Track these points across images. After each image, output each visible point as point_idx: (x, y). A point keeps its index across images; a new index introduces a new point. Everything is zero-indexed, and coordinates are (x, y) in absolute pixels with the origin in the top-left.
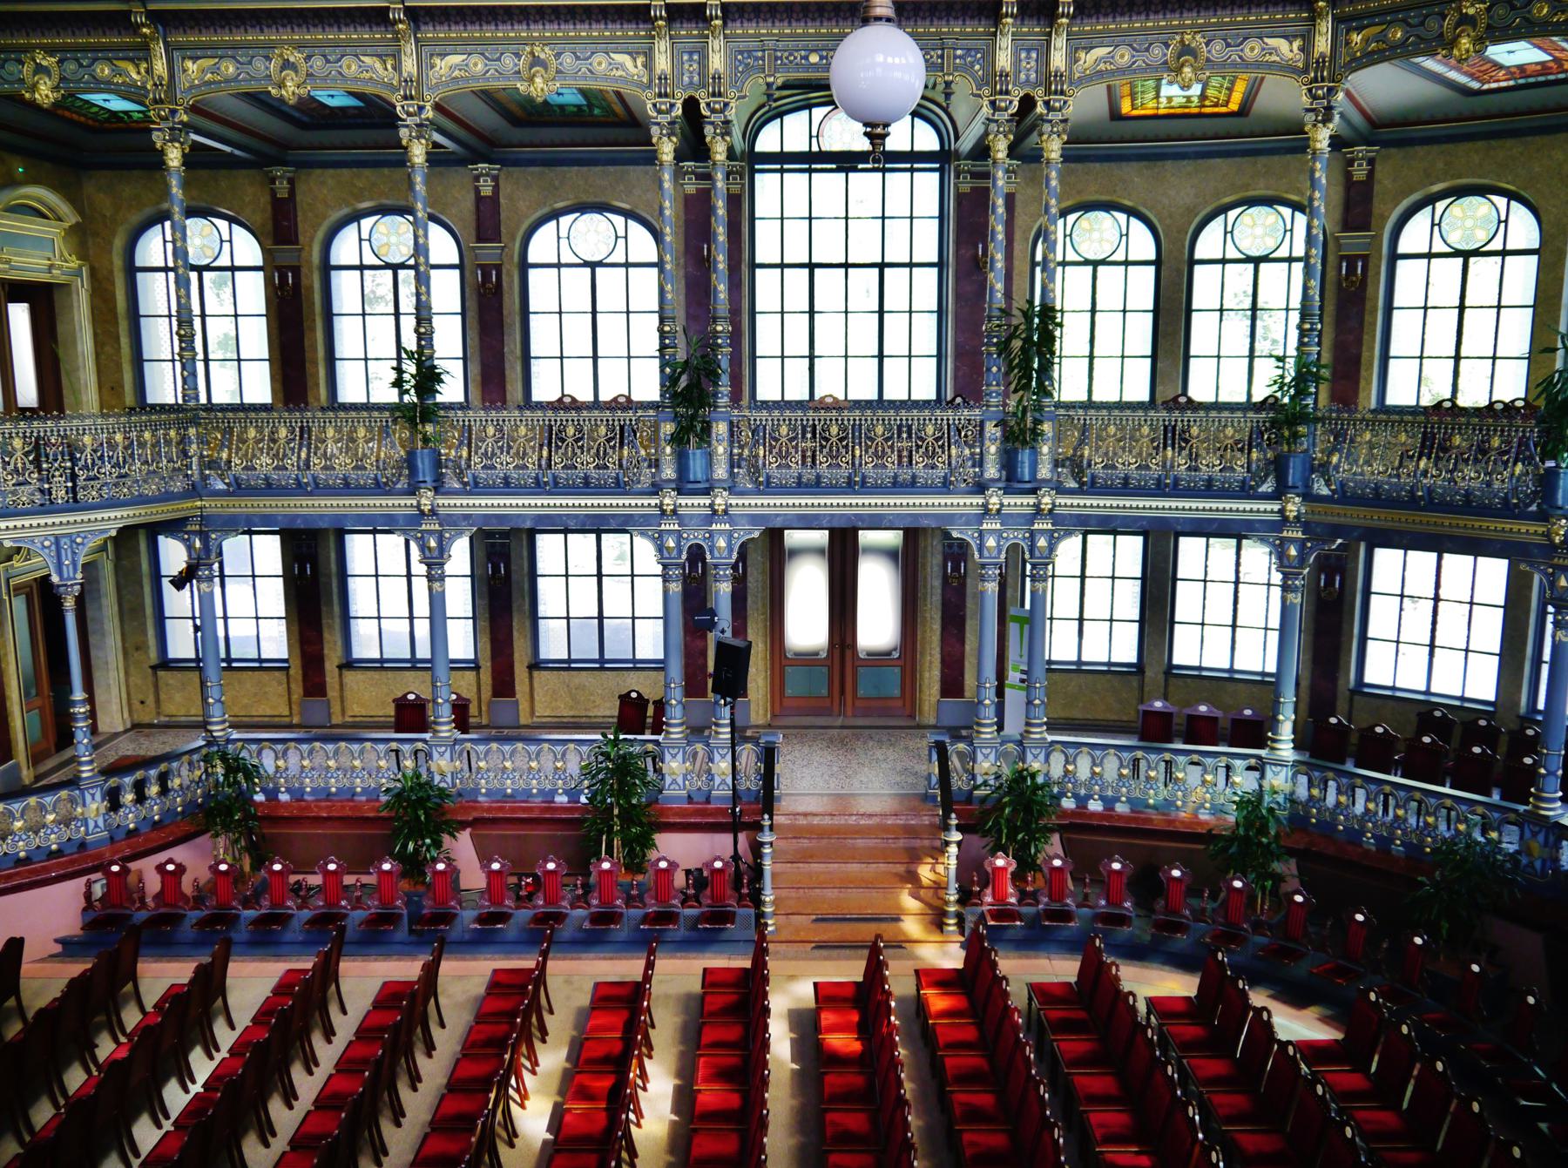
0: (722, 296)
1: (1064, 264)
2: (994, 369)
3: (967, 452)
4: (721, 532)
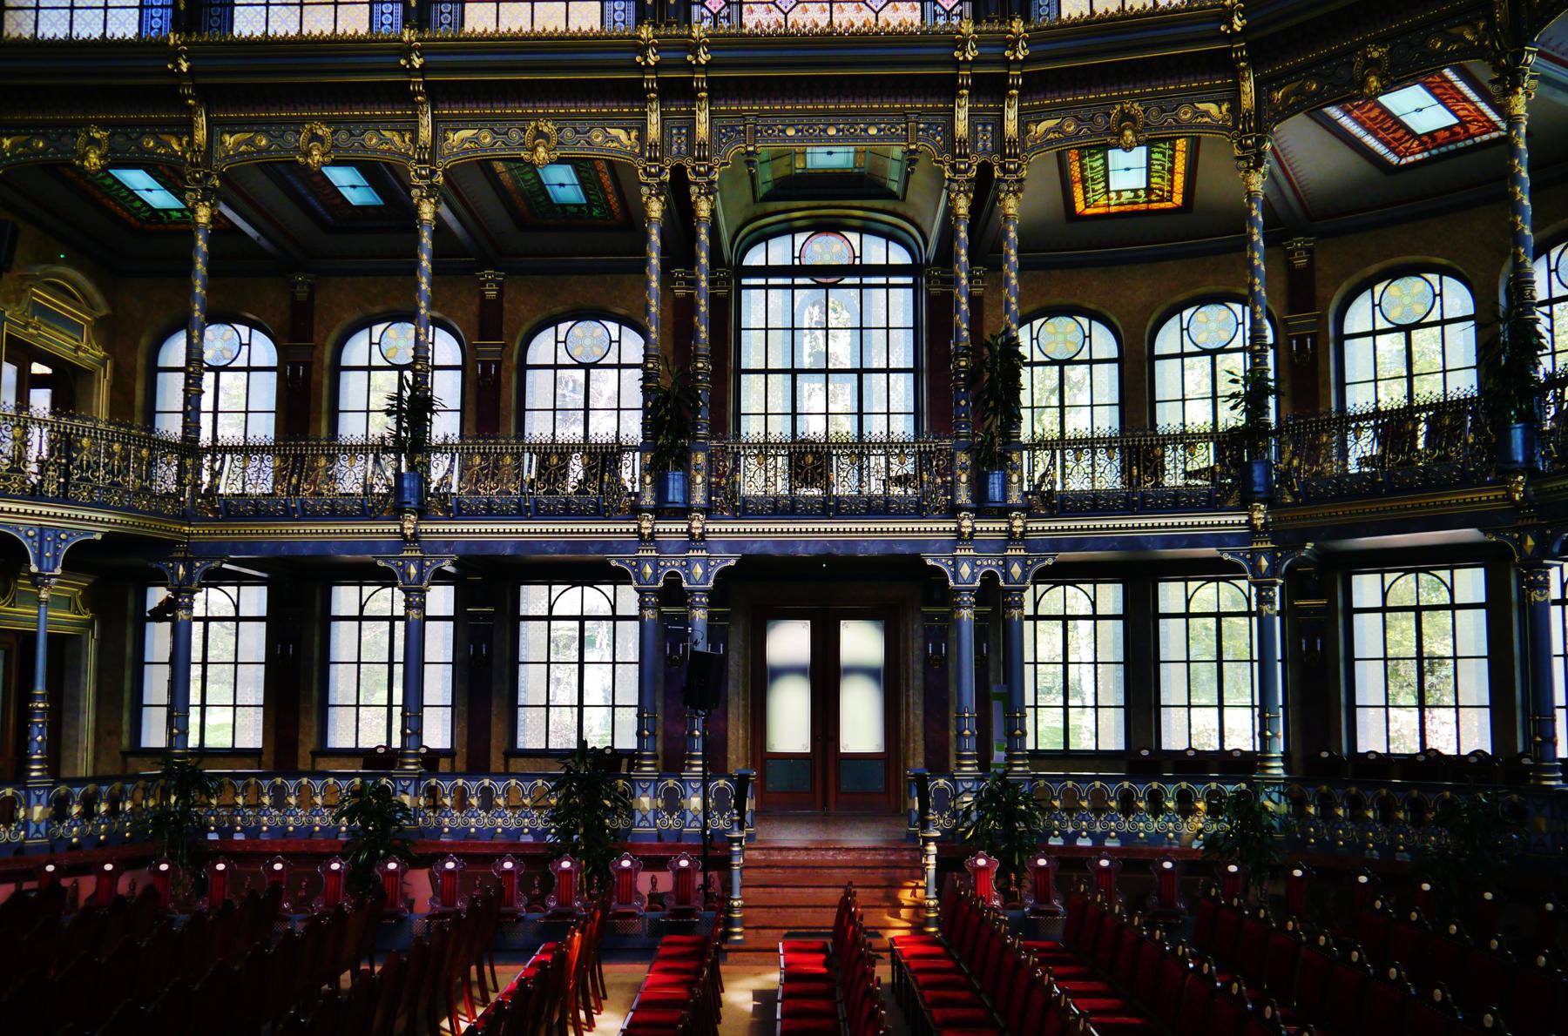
0: (703, 336)
2: (963, 403)
3: (939, 480)
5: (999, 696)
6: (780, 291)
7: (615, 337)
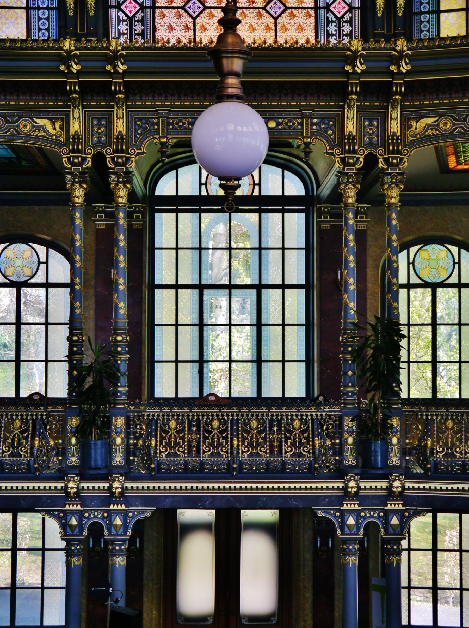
0: (122, 312)
1: (409, 286)
2: (350, 373)
3: (328, 442)
4: (118, 512)
5: (378, 588)
7: (43, 259)
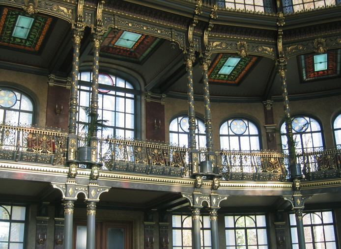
6: (85, 93)
